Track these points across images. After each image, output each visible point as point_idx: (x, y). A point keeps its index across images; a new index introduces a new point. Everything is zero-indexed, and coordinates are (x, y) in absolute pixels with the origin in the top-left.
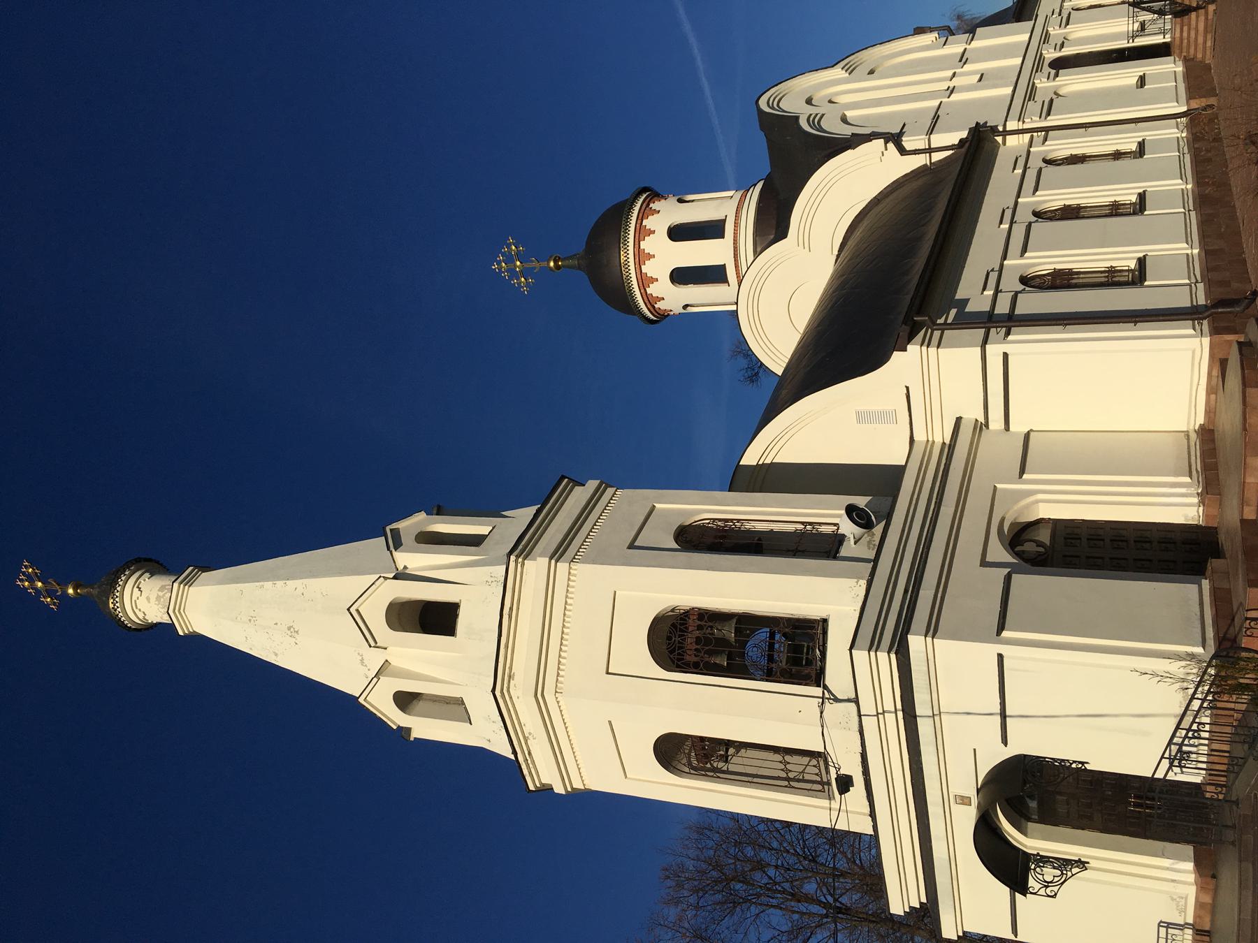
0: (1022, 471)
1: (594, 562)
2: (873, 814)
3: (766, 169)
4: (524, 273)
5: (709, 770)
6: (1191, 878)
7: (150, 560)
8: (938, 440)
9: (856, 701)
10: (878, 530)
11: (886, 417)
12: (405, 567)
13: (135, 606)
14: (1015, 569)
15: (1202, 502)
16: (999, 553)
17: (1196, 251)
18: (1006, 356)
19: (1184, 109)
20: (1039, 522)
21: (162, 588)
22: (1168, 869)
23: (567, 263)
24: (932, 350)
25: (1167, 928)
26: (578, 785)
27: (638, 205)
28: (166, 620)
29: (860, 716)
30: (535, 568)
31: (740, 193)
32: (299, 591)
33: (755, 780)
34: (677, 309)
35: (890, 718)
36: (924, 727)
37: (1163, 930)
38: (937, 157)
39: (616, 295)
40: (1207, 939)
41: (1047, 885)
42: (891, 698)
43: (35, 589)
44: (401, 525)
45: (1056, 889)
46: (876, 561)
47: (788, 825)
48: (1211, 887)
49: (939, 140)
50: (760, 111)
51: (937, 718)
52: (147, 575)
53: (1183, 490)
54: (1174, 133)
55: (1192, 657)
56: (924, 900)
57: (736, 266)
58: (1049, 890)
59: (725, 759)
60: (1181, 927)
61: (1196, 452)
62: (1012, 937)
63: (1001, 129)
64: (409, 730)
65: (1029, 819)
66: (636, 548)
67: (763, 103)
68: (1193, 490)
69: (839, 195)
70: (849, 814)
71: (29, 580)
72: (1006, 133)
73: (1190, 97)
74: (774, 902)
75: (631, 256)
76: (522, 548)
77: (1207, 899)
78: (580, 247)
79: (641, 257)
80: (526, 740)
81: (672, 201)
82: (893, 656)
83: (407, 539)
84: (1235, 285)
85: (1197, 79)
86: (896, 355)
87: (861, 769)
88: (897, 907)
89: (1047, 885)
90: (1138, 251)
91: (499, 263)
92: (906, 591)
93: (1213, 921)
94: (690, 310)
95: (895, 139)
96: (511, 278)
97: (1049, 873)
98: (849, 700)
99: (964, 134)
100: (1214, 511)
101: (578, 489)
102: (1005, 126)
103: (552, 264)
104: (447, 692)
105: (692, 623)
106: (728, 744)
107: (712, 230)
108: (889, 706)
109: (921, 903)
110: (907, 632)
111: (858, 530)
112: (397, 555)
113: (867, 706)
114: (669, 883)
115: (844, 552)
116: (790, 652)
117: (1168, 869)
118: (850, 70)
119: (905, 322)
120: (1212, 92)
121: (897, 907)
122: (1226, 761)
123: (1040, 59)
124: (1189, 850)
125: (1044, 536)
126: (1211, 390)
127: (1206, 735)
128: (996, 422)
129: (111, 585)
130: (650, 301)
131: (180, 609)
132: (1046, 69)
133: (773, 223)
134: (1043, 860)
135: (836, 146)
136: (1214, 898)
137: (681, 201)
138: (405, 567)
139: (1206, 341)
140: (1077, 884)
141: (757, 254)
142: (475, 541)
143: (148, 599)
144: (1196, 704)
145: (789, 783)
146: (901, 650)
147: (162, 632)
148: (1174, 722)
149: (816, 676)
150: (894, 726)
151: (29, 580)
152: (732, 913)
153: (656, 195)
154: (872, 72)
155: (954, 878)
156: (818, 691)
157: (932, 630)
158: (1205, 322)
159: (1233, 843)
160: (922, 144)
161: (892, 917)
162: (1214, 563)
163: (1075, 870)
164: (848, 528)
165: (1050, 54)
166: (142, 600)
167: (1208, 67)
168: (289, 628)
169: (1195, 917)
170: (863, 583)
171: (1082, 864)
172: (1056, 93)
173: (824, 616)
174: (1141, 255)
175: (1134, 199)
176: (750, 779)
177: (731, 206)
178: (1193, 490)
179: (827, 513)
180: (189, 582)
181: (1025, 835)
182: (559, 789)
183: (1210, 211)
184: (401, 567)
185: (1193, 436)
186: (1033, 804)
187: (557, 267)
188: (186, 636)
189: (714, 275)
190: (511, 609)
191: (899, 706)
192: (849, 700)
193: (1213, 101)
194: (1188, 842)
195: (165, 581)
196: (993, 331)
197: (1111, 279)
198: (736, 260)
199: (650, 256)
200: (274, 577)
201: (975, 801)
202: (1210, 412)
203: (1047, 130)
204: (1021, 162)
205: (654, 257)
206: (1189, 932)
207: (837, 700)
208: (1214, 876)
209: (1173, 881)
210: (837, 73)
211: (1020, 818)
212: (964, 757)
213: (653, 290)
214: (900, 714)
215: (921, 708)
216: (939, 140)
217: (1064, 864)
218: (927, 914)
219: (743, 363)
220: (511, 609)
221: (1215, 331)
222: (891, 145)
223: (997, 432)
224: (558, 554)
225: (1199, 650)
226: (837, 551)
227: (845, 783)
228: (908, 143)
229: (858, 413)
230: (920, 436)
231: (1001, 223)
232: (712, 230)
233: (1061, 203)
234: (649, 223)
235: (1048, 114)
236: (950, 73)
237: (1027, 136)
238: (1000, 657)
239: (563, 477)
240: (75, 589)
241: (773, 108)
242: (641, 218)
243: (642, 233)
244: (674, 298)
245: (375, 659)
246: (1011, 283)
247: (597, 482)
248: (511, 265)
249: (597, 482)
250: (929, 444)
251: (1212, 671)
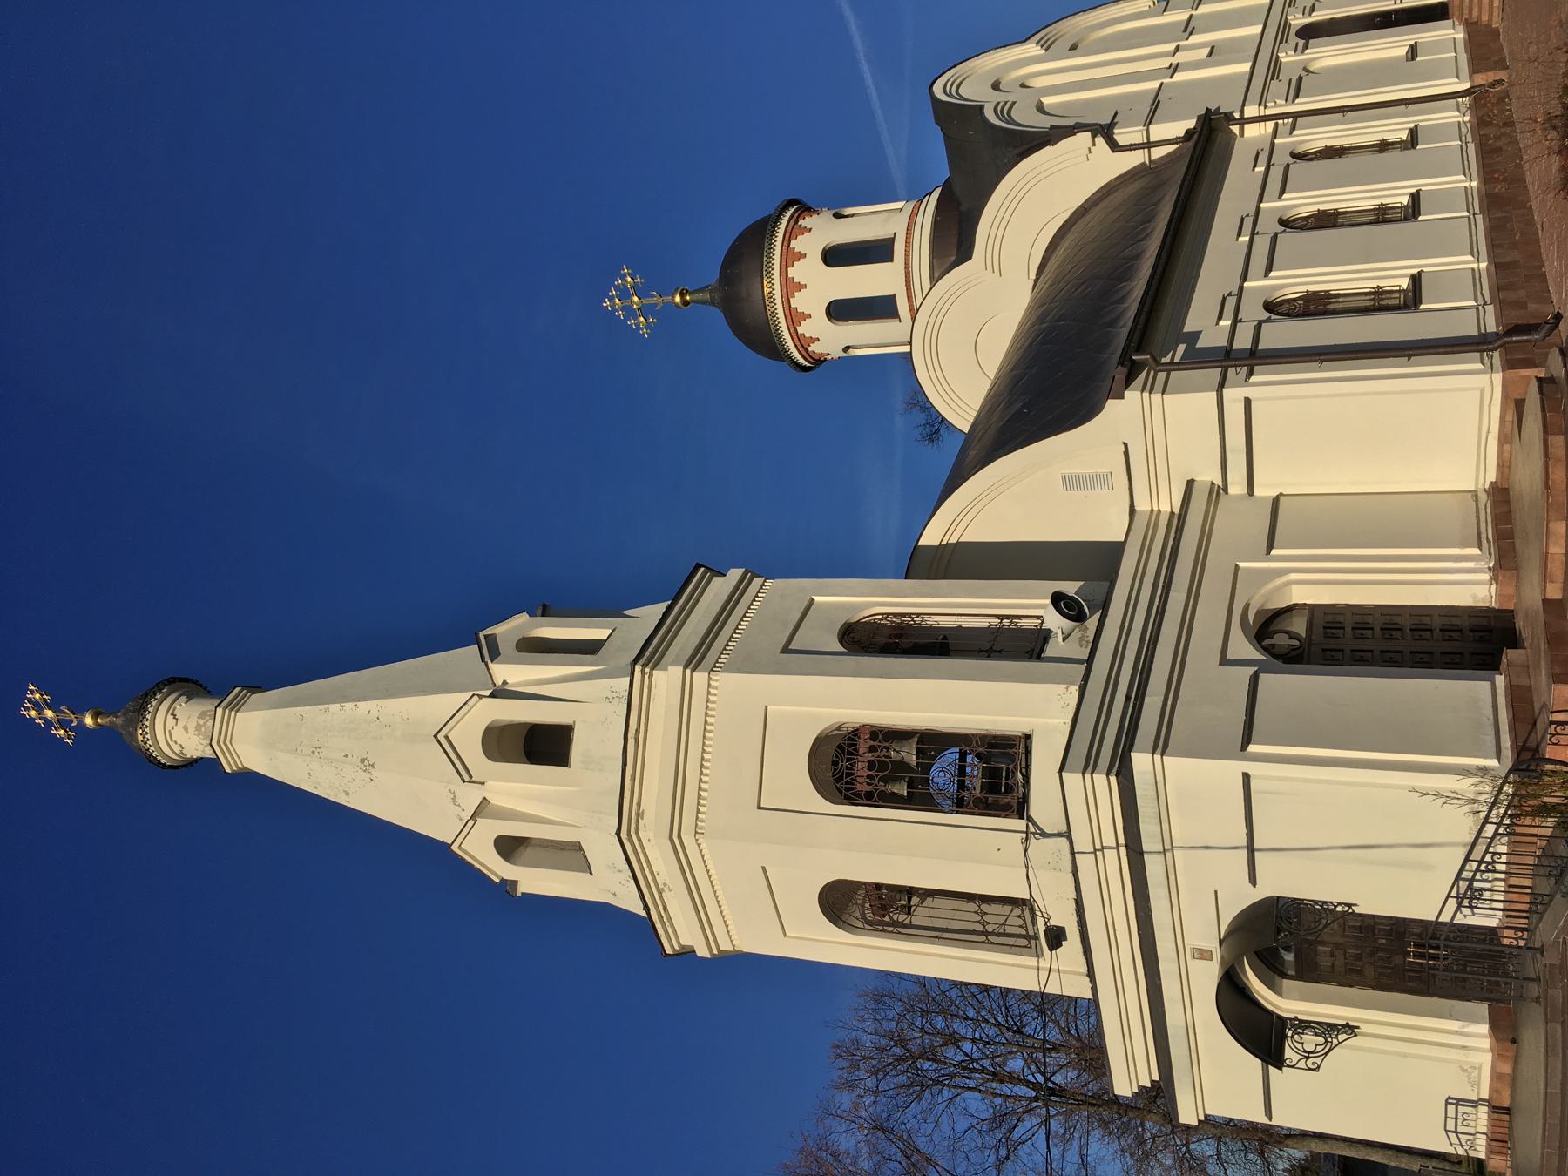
0: (1270, 545)
1: (739, 671)
2: (1091, 974)
4: (645, 311)
5: (888, 925)
6: (1486, 1043)
7: (186, 680)
8: (1165, 508)
9: (1068, 835)
10: (1092, 623)
11: (1101, 482)
12: (505, 683)
13: (169, 738)
14: (1262, 668)
15: (1495, 579)
16: (1242, 647)
17: (1483, 265)
18: (1248, 402)
19: (1466, 86)
20: (1291, 609)
21: (202, 715)
22: (1456, 1033)
23: (696, 296)
24: (1156, 397)
25: (1457, 1105)
26: (726, 946)
28: (208, 753)
29: (1073, 853)
30: (667, 679)
31: (912, 204)
32: (375, 713)
33: (946, 935)
34: (836, 352)
35: (1111, 855)
36: (1153, 866)
37: (1451, 1108)
38: (1158, 153)
39: (762, 340)
40: (1506, 1117)
41: (1307, 1055)
42: (1111, 829)
43: (46, 719)
44: (498, 630)
45: (1318, 1060)
46: (1090, 661)
47: (986, 989)
48: (1511, 1054)
49: (1160, 131)
50: (935, 100)
51: (1168, 854)
52: (184, 698)
53: (1471, 565)
54: (1454, 116)
55: (1484, 771)
56: (1156, 1077)
57: (909, 297)
58: (1310, 1062)
59: (908, 910)
60: (1474, 1104)
61: (1487, 515)
62: (1265, 1120)
63: (1237, 115)
64: (515, 883)
65: (1284, 975)
66: (791, 653)
67: (938, 90)
68: (1483, 565)
69: (1035, 205)
70: (1061, 974)
71: (37, 709)
72: (1243, 121)
73: (1475, 68)
74: (971, 1083)
75: (777, 286)
76: (649, 654)
77: (1506, 1068)
78: (713, 276)
79: (790, 288)
80: (660, 892)
81: (827, 215)
82: (1113, 779)
83: (506, 647)
84: (1532, 306)
85: (1482, 48)
86: (1112, 405)
87: (1074, 919)
88: (1123, 1087)
89: (1307, 1055)
90: (1412, 266)
91: (611, 299)
92: (1128, 698)
93: (1513, 1097)
94: (853, 352)
95: (1105, 131)
96: (627, 318)
97: (1310, 1041)
98: (1059, 835)
99: (1191, 124)
100: (1511, 590)
101: (717, 580)
102: (1242, 112)
103: (678, 299)
104: (565, 834)
105: (863, 744)
106: (910, 891)
107: (877, 251)
108: (1109, 840)
109: (1152, 1082)
110: (1130, 746)
111: (1067, 624)
112: (494, 667)
113: (1082, 841)
114: (842, 1063)
115: (1049, 651)
116: (989, 776)
117: (1456, 1033)
118: (1047, 45)
119: (1121, 363)
120: (1501, 64)
121: (1123, 1087)
122: (1527, 899)
123: (1284, 27)
124: (1483, 1008)
125: (1299, 626)
126: (1504, 439)
127: (1503, 867)
128: (1237, 487)
129: (141, 710)
130: (802, 343)
131: (226, 740)
132: (1293, 39)
133: (955, 239)
134: (1302, 1025)
135: (1030, 142)
136: (1514, 1070)
137: (837, 216)
138: (505, 683)
139: (1498, 377)
140: (1345, 1054)
141: (934, 280)
142: (590, 648)
143: (186, 728)
144: (1489, 830)
145: (987, 937)
146: (1123, 771)
147: (201, 772)
148: (1464, 851)
149: (1020, 808)
150: (1115, 865)
151: (37, 709)
152: (919, 1098)
153: (806, 209)
154: (1074, 47)
155: (1192, 1051)
156: (1021, 824)
157: (1161, 745)
158: (1496, 354)
159: (1537, 1000)
160: (1138, 138)
161: (1116, 1100)
162: (1510, 655)
163: (1342, 1037)
164: (1055, 621)
166: (177, 729)
167: (1495, 33)
168: (362, 761)
169: (1493, 1090)
170: (1075, 689)
171: (1350, 1029)
172: (1305, 69)
173: (1027, 731)
174: (1415, 271)
175: (1405, 200)
176: (938, 934)
177: (902, 221)
178: (1483, 565)
179: (1029, 603)
180: (236, 706)
181: (1280, 994)
182: (702, 952)
183: (1499, 215)
184: (499, 682)
185: (1483, 497)
186: (1289, 957)
187: (686, 303)
188: (235, 775)
189: (880, 308)
190: (638, 731)
191: (1121, 840)
192: (1059, 835)
193: (1501, 75)
194: (1482, 1000)
195: (207, 705)
196: (1231, 371)
197: (1379, 302)
198: (908, 289)
199: (800, 287)
200: (342, 697)
201: (1217, 955)
202: (1504, 466)
203: (1295, 116)
204: (1263, 157)
205: (806, 287)
206: (1484, 1110)
207: (1044, 835)
208: (1514, 1041)
209: (1464, 1047)
210: (1031, 49)
211: (1272, 970)
212: (1202, 904)
213: (805, 329)
214: (1123, 851)
215: (1149, 843)
216: (1160, 131)
217: (1329, 1030)
218: (1159, 1095)
219: (921, 418)
220: (638, 731)
221: (1509, 364)
222: (1100, 140)
223: (1236, 497)
224: (694, 661)
225: (1493, 763)
226: (1042, 651)
227: (1056, 937)
228: (1123, 136)
229: (1064, 477)
230: (1142, 505)
231: (1239, 234)
232: (877, 251)
233: (1315, 208)
234: (798, 244)
235: (1297, 96)
236: (1172, 47)
237: (1270, 125)
238: (1246, 776)
239: (698, 566)
240: (95, 717)
241: (950, 95)
243: (790, 257)
244: (830, 339)
245: (471, 798)
246: (1253, 310)
247: (740, 571)
248: (627, 300)
249: (740, 571)
250: (1154, 515)
251: (1508, 789)
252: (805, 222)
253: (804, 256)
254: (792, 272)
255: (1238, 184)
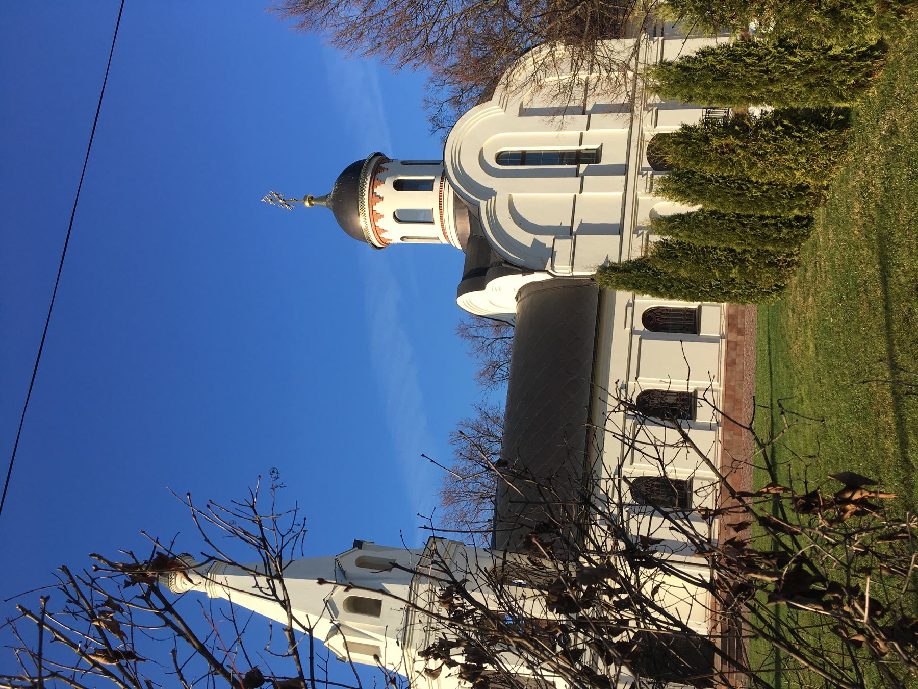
27: (366, 193)
118: (504, 106)
132: (646, 164)
165: (650, 133)
183: (728, 438)
199: (384, 231)
234: (378, 207)
236: (578, 133)
241: (455, 171)
242: (371, 205)
253: (382, 216)
254: (377, 224)
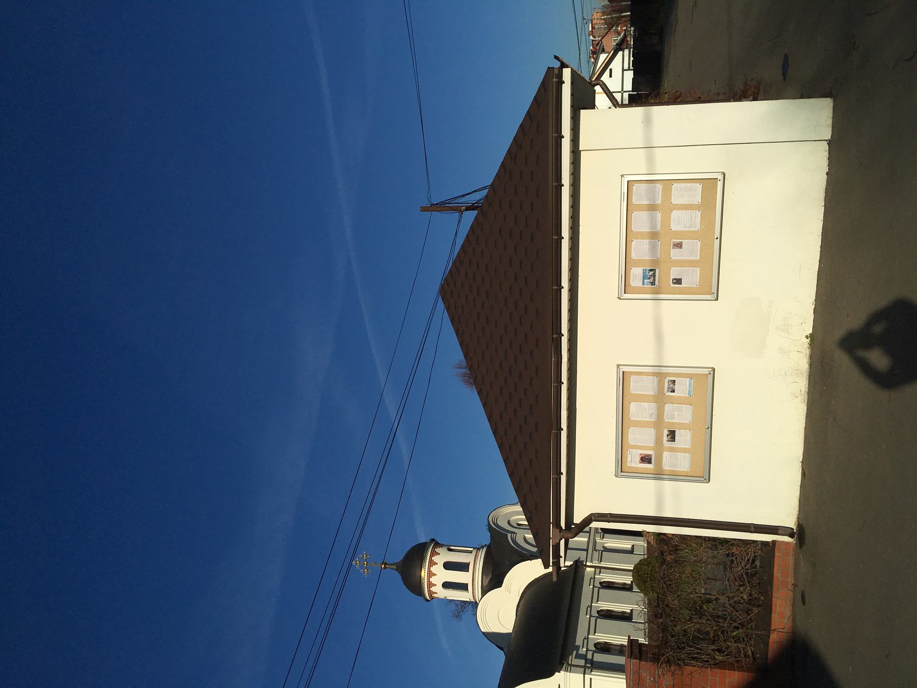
3: (488, 542)
31: (474, 552)
39: (415, 587)
79: (431, 574)
130: (431, 593)
137: (450, 550)
153: (437, 545)
177: (477, 562)
187: (385, 568)
189: (463, 587)
205: (436, 575)
213: (433, 589)
219: (453, 607)
232: (463, 567)
234: (435, 559)
242: (431, 556)
243: (432, 563)
252: (437, 550)
255: (587, 589)
